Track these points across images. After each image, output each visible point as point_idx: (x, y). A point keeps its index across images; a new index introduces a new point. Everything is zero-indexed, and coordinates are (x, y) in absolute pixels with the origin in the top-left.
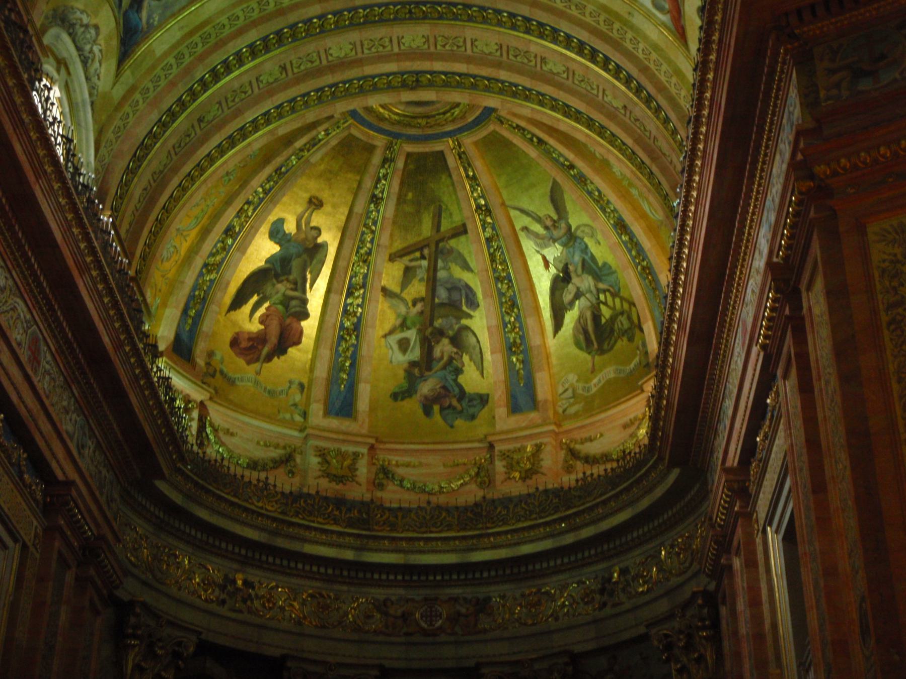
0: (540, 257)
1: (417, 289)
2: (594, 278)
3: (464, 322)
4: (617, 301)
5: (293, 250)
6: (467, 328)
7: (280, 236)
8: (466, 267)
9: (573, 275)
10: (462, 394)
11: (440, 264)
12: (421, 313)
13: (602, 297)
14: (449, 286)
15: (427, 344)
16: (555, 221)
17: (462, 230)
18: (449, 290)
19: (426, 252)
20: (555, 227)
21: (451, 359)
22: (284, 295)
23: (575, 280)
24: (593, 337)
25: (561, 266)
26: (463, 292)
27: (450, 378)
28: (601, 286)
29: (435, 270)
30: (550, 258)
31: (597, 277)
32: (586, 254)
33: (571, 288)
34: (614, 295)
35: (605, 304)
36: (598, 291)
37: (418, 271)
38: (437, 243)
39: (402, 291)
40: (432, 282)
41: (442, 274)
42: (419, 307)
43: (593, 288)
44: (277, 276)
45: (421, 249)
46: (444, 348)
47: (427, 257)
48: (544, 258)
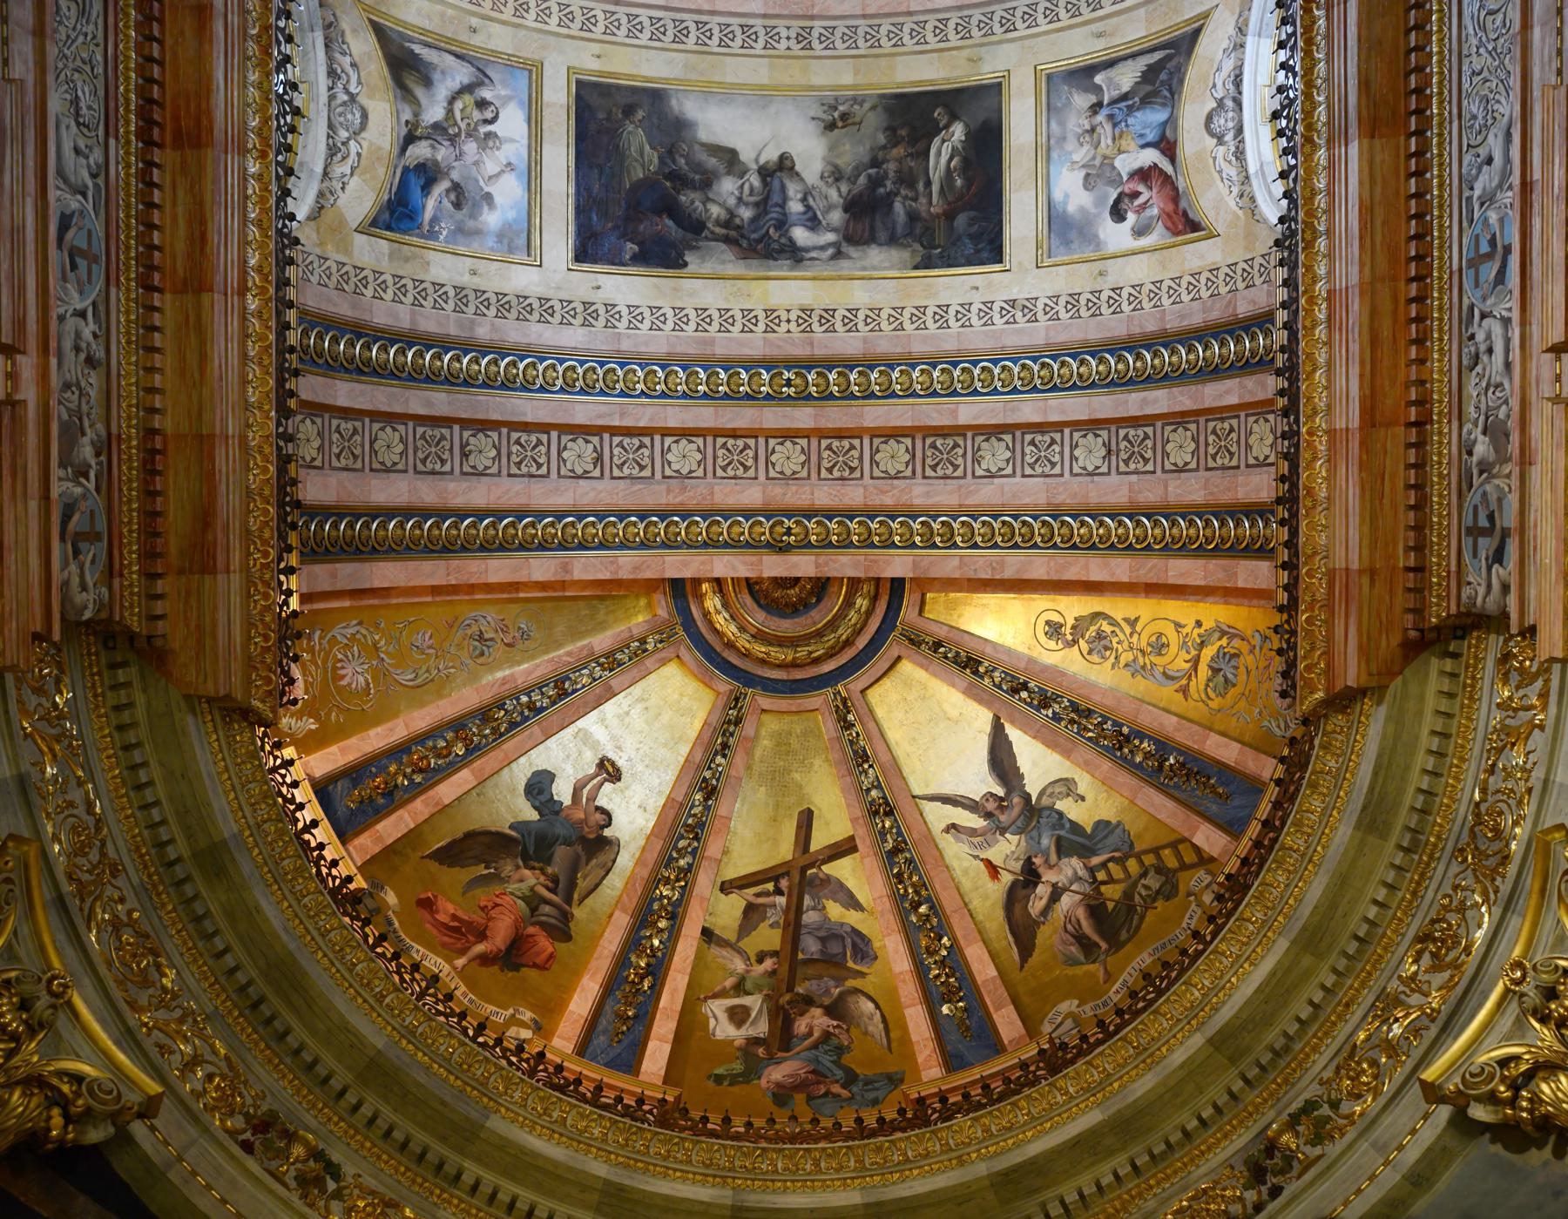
0: (981, 865)
1: (768, 936)
2: (1080, 857)
3: (851, 983)
4: (1132, 864)
5: (560, 830)
6: (857, 991)
7: (543, 798)
8: (852, 903)
9: (1041, 870)
10: (850, 1078)
11: (807, 901)
12: (773, 973)
13: (1101, 876)
14: (822, 934)
15: (783, 1020)
16: (1002, 799)
17: (845, 848)
18: (823, 940)
19: (784, 883)
20: (1001, 808)
21: (827, 1036)
22: (532, 889)
23: (1049, 876)
24: (1096, 938)
25: (1018, 866)
26: (848, 942)
27: (826, 1060)
28: (1096, 860)
29: (799, 911)
30: (997, 861)
31: (1085, 851)
32: (1062, 827)
33: (1042, 890)
34: (1121, 861)
35: (1111, 880)
36: (1092, 871)
37: (770, 912)
38: (804, 870)
39: (739, 939)
40: (793, 927)
41: (810, 917)
42: (768, 964)
43: (1082, 873)
44: (526, 858)
45: (776, 879)
46: (814, 1021)
47: (786, 891)
48: (988, 863)
